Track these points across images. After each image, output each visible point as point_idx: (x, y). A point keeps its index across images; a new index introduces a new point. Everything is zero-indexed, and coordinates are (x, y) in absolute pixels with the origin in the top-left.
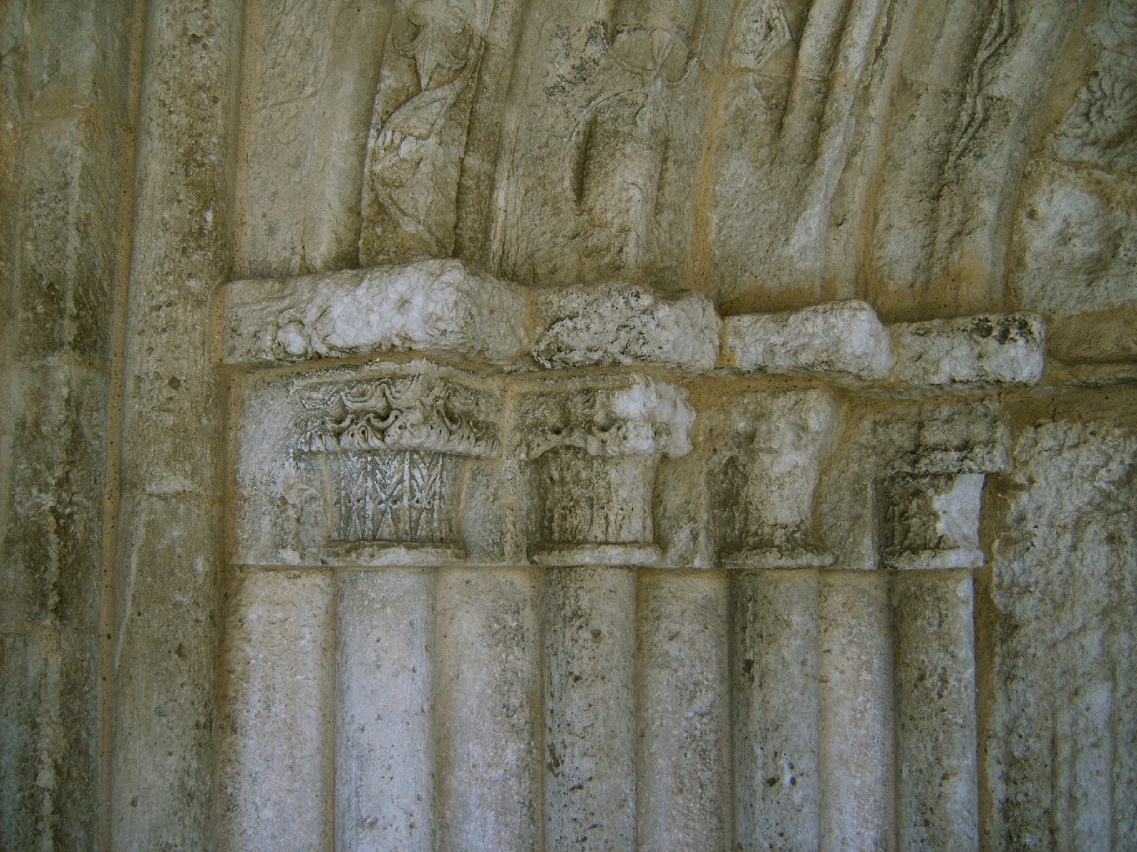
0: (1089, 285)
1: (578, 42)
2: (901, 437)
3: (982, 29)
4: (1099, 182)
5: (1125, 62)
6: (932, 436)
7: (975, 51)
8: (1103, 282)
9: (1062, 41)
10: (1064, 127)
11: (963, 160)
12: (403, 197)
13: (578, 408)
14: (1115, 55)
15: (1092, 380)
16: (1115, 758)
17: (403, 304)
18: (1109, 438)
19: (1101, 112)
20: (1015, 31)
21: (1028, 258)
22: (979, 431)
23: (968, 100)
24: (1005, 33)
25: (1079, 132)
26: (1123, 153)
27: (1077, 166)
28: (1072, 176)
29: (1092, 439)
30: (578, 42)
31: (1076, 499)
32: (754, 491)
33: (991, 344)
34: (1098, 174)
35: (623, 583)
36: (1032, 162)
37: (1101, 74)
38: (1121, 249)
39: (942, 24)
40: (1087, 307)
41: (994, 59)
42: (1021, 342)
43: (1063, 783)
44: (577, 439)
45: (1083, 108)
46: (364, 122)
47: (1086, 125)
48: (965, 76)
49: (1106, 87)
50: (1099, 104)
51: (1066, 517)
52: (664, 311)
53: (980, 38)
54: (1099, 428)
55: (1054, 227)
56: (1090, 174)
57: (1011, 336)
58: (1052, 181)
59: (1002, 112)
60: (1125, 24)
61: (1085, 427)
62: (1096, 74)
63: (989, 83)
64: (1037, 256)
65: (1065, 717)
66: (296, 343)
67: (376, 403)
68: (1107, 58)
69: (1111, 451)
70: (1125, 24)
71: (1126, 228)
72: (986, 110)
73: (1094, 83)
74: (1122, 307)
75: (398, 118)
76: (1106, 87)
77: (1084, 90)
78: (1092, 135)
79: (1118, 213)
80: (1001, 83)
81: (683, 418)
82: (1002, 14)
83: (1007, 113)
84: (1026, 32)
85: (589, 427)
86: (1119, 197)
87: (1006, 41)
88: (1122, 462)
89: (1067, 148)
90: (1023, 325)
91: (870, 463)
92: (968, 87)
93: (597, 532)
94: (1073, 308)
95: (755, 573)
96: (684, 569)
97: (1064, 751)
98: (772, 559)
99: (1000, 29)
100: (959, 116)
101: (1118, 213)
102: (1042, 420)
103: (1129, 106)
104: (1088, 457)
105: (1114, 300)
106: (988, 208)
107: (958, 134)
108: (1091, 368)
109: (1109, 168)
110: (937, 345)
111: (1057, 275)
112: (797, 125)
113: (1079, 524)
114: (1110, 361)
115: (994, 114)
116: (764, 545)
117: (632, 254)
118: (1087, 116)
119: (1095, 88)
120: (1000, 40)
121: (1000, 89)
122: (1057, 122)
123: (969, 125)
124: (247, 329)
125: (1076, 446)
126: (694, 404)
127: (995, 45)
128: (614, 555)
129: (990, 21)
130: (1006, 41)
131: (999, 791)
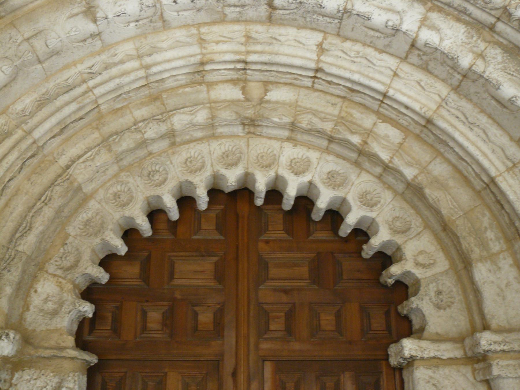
0: (51, 319)
3: (20, 226)
4: (60, 283)
5: (76, 242)
7: (16, 232)
8: (55, 319)
9: (55, 232)
10: (52, 261)
11: (3, 272)
14: (73, 239)
15: (42, 355)
18: (48, 377)
19: (66, 258)
20: (30, 229)
21: (31, 308)
23: (10, 250)
24: (27, 228)
25: (57, 263)
26: (70, 273)
27: (55, 276)
28: (52, 279)
29: (43, 377)
34: (60, 280)
36: (39, 272)
37: (68, 244)
38: (63, 308)
39: (7, 222)
40: (49, 327)
41: (21, 237)
42: (6, 341)
45: (61, 255)
47: (61, 261)
48: (10, 241)
49: (70, 248)
50: (66, 255)
53: (18, 229)
54: (45, 372)
55: (44, 296)
56: (58, 279)
57: (2, 338)
58: (45, 280)
59: (20, 257)
60: (79, 228)
61: (41, 372)
62: (66, 244)
63: (18, 246)
64: (35, 307)
68: (71, 239)
69: (48, 382)
70: (79, 228)
71: (66, 300)
72: (15, 255)
73: (66, 247)
74: (60, 329)
76: (70, 248)
77: (62, 249)
78: (62, 266)
79: (65, 295)
80: (22, 246)
82: (27, 222)
83: (21, 257)
84: (34, 229)
86: (66, 289)
87: (27, 231)
88: (52, 386)
89: (51, 268)
90: (7, 335)
92: (10, 246)
94: (43, 327)
99: (26, 227)
100: (6, 256)
101: (65, 295)
102: (25, 368)
103: (76, 257)
104: (40, 383)
105: (58, 326)
107: (3, 262)
108: (43, 350)
109: (64, 278)
111: (41, 314)
114: (51, 348)
115: (17, 257)
118: (61, 258)
119: (66, 249)
120: (25, 231)
121: (20, 248)
122: (50, 259)
123: (8, 260)
125: (36, 379)
127: (23, 232)
129: (23, 224)
130: (27, 231)
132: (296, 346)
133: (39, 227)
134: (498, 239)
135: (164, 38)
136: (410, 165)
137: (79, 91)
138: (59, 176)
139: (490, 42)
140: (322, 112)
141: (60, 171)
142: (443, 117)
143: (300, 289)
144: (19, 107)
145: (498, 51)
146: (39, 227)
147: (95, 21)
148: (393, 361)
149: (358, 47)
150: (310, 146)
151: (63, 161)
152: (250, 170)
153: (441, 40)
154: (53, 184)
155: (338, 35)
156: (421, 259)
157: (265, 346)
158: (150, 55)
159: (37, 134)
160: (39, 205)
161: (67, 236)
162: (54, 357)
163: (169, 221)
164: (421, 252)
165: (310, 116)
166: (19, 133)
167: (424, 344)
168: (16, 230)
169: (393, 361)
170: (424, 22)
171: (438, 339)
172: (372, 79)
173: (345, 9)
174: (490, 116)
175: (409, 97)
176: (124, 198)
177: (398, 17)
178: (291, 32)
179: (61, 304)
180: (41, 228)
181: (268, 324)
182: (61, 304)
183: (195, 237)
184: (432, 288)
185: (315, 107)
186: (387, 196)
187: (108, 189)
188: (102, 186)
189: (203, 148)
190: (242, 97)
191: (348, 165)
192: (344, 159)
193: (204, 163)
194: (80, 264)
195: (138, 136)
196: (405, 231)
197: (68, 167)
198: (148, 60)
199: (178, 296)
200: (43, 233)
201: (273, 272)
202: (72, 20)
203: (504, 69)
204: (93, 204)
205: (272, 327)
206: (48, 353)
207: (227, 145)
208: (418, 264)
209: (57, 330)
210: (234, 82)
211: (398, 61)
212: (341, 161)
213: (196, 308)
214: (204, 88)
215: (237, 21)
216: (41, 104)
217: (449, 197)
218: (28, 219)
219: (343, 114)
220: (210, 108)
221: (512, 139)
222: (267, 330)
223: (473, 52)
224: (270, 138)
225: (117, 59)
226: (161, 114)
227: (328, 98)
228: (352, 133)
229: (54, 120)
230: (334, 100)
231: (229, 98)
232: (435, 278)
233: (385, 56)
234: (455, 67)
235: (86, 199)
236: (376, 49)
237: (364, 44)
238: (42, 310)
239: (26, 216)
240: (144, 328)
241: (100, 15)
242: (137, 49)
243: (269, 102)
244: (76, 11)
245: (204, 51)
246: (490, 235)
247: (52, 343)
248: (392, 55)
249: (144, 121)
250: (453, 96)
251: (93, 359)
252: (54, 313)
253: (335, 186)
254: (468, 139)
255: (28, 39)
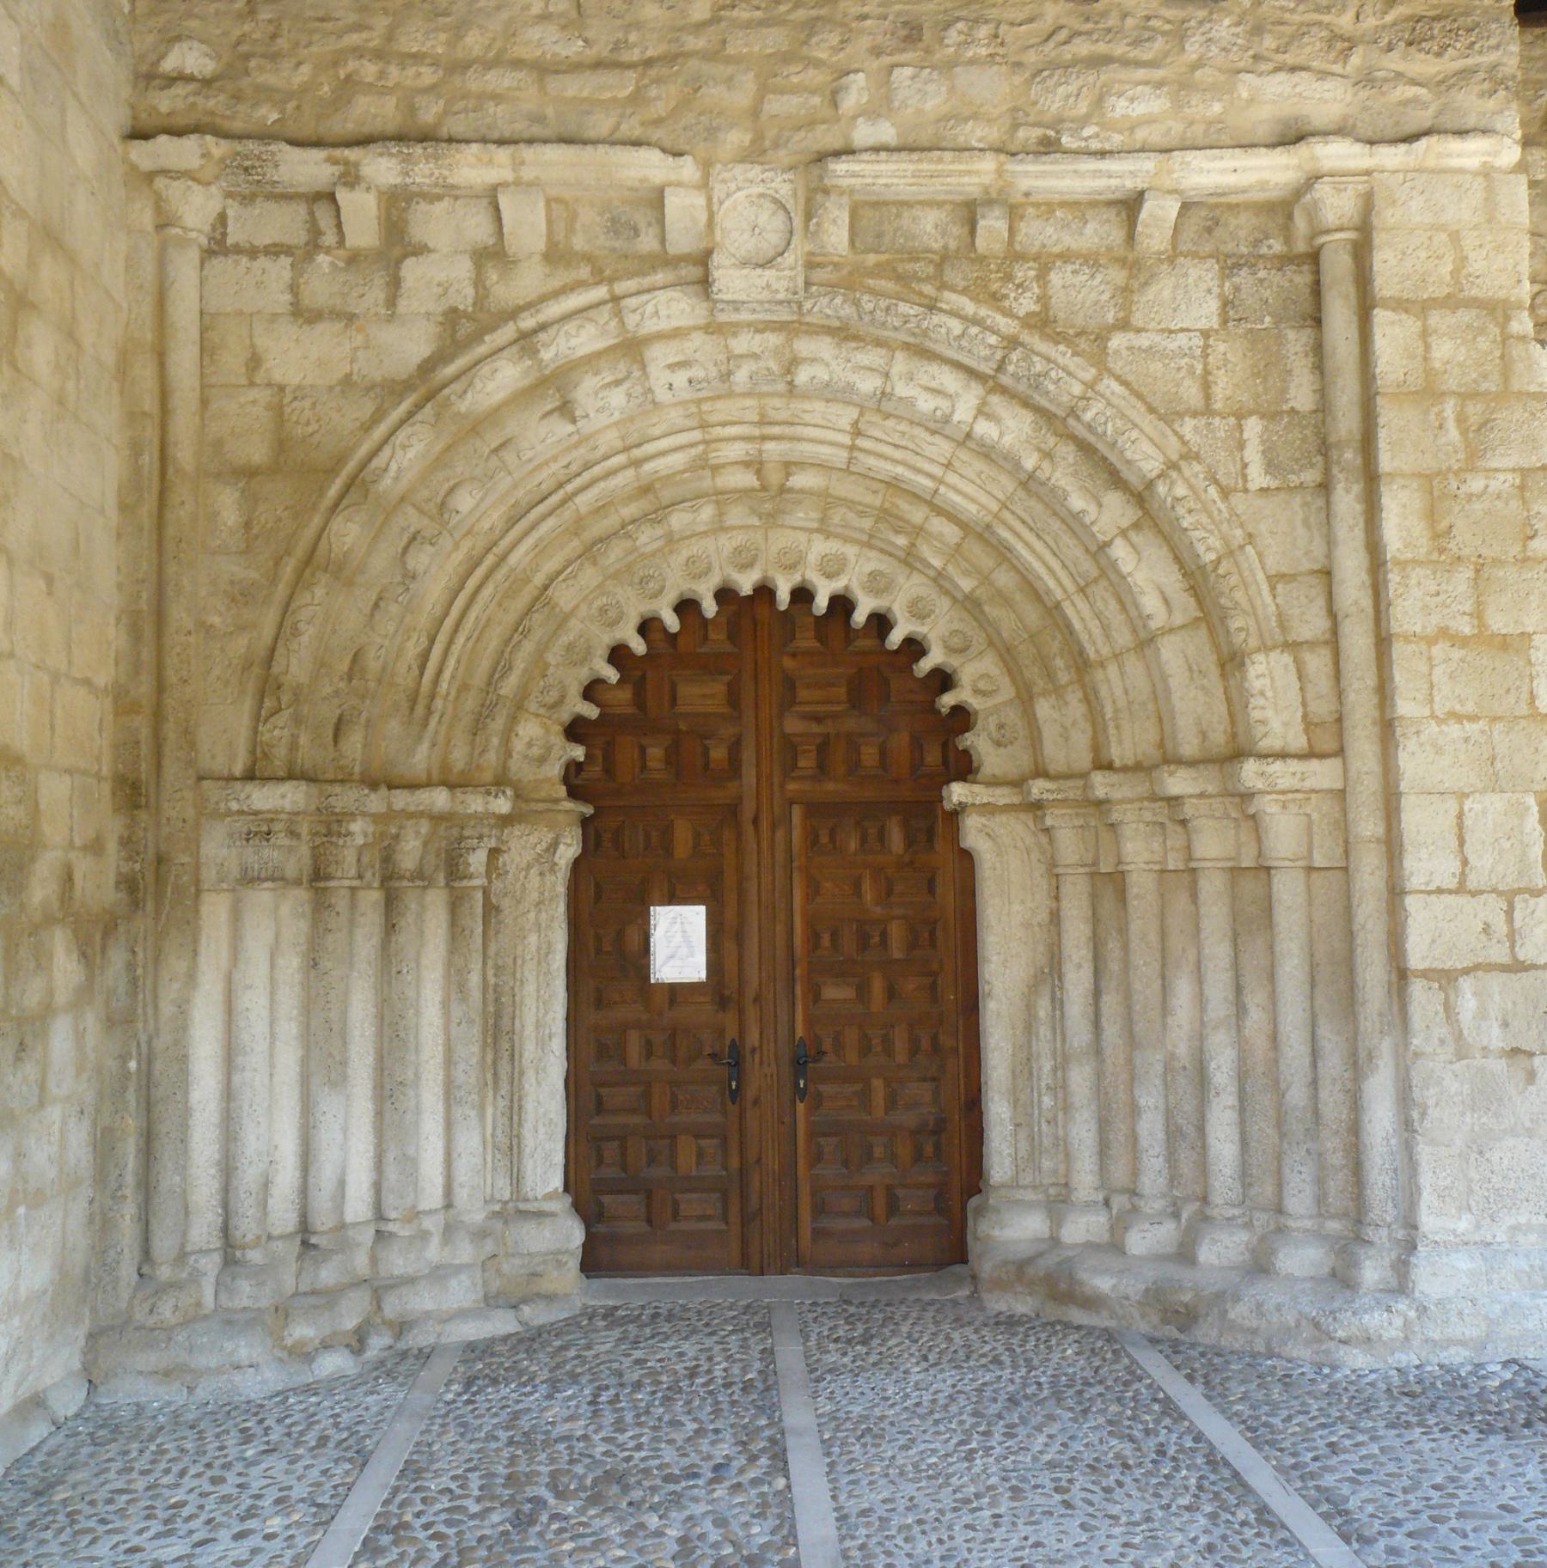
1: (335, 680)
2: (455, 832)
6: (467, 833)
12: (275, 751)
13: (335, 827)
16: (539, 963)
17: (283, 797)
20: (510, 668)
21: (515, 755)
22: (486, 831)
27: (538, 715)
30: (335, 680)
31: (528, 856)
32: (398, 857)
33: (491, 798)
35: (344, 892)
43: (518, 976)
44: (334, 839)
46: (257, 718)
48: (489, 684)
51: (524, 865)
52: (373, 796)
65: (520, 948)
66: (235, 806)
67: (265, 828)
68: (551, 670)
75: (272, 719)
81: (371, 829)
85: (339, 835)
89: (533, 706)
91: (444, 844)
93: (339, 874)
94: (531, 777)
95: (397, 889)
96: (369, 887)
97: (519, 962)
98: (405, 883)
104: (533, 839)
106: (495, 741)
110: (470, 798)
112: (420, 710)
113: (529, 867)
114: (544, 801)
116: (401, 878)
117: (357, 769)
121: (502, 692)
124: (214, 799)
126: (375, 822)
128: (347, 883)
131: (492, 980)
132: (830, 786)
133: (520, 665)
134: (1068, 668)
135: (655, 420)
136: (966, 573)
137: (554, 499)
138: (537, 599)
139: (1061, 436)
140: (860, 504)
141: (536, 593)
142: (1004, 523)
143: (834, 716)
144: (486, 525)
145: (1072, 448)
146: (520, 665)
147: (574, 421)
148: (947, 806)
149: (903, 427)
150: (846, 540)
151: (539, 579)
152: (770, 574)
153: (1001, 435)
154: (529, 611)
155: (879, 410)
156: (982, 685)
157: (792, 786)
158: (639, 445)
159: (513, 559)
160: (516, 637)
161: (547, 665)
162: (549, 810)
163: (664, 630)
164: (982, 676)
165: (844, 510)
166: (490, 560)
167: (976, 788)
168: (494, 670)
169: (947, 806)
170: (982, 411)
171: (994, 782)
172: (919, 471)
173: (883, 393)
174: (1063, 521)
175: (965, 496)
176: (612, 614)
177: (949, 404)
178: (819, 406)
179: (549, 749)
180: (522, 666)
181: (795, 759)
182: (549, 749)
183: (702, 650)
184: (992, 723)
185: (851, 496)
186: (944, 604)
187: (591, 604)
188: (584, 599)
189: (709, 544)
190: (756, 484)
191: (896, 563)
192: (891, 555)
193: (710, 563)
194: (567, 700)
195: (628, 544)
196: (962, 650)
197: (546, 587)
198: (637, 453)
199: (683, 727)
200: (525, 670)
201: (803, 694)
202: (545, 422)
203: (1075, 474)
204: (575, 625)
205: (802, 763)
206: (541, 806)
207: (739, 538)
208: (977, 691)
209: (547, 780)
210: (746, 464)
211: (953, 445)
212: (886, 558)
213: (707, 742)
214: (707, 473)
215: (747, 395)
216: (512, 521)
217: (1013, 616)
218: (506, 655)
219: (887, 505)
220: (717, 502)
221: (1087, 551)
222: (795, 766)
223: (1039, 450)
224: (794, 528)
225: (599, 453)
226: (655, 512)
227: (868, 482)
228: (897, 532)
229: (530, 541)
230: (876, 486)
231: (740, 485)
232: (996, 709)
233: (937, 439)
234: (1018, 466)
235: (566, 618)
236: (927, 429)
237: (912, 423)
238: (526, 757)
239: (503, 652)
240: (644, 767)
241: (578, 413)
242: (623, 438)
243: (791, 490)
244: (549, 407)
245: (707, 437)
246: (1059, 663)
247: (543, 794)
248: (947, 437)
249: (634, 521)
250: (1021, 493)
251: (588, 810)
252: (542, 760)
253: (876, 592)
254: (1034, 551)
255: (496, 450)
